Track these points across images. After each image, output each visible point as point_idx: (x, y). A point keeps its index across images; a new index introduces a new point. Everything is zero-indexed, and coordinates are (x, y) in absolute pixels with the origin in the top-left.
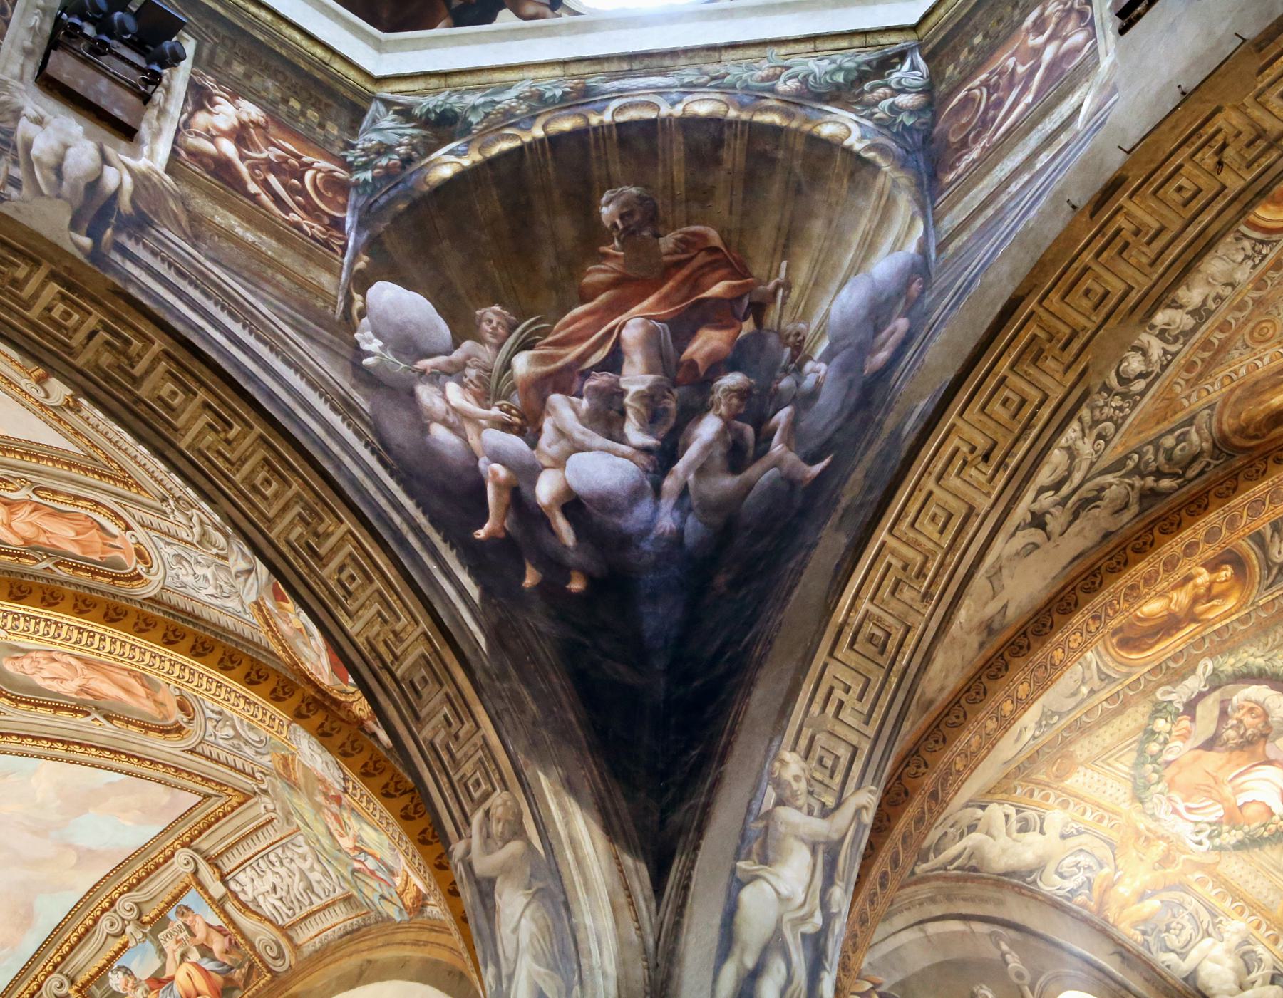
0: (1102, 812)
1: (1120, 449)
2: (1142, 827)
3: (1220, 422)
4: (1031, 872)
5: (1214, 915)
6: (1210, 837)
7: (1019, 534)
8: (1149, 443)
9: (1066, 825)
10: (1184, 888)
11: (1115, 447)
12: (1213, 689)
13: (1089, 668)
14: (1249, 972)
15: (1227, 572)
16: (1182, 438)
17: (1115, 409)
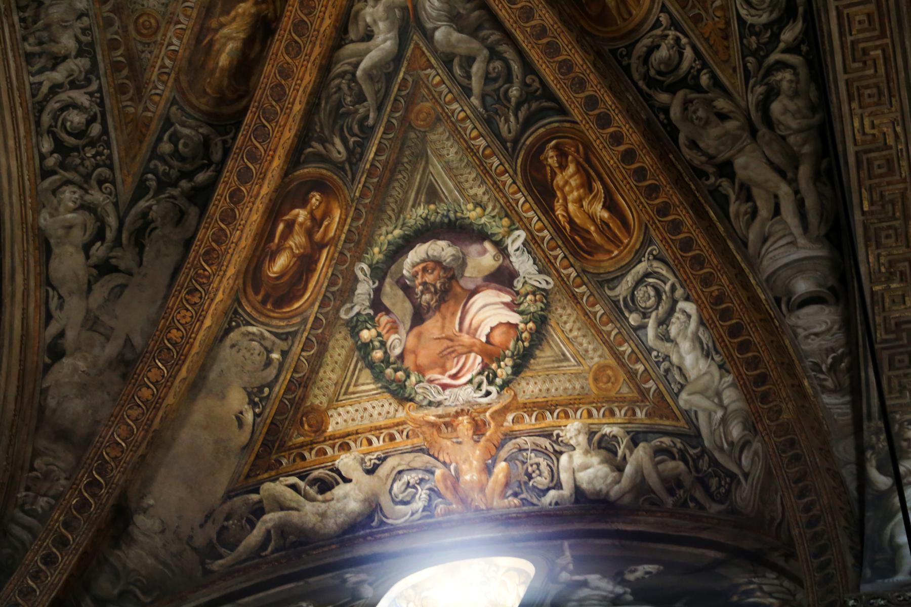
0: (385, 432)
1: (130, 179)
2: (432, 419)
3: (193, 107)
4: (370, 516)
5: (549, 436)
6: (491, 383)
7: (96, 287)
8: (150, 160)
9: (362, 461)
10: (510, 436)
11: (123, 182)
12: (382, 281)
13: (262, 337)
14: (616, 454)
15: (315, 199)
16: (175, 139)
17: (94, 156)
